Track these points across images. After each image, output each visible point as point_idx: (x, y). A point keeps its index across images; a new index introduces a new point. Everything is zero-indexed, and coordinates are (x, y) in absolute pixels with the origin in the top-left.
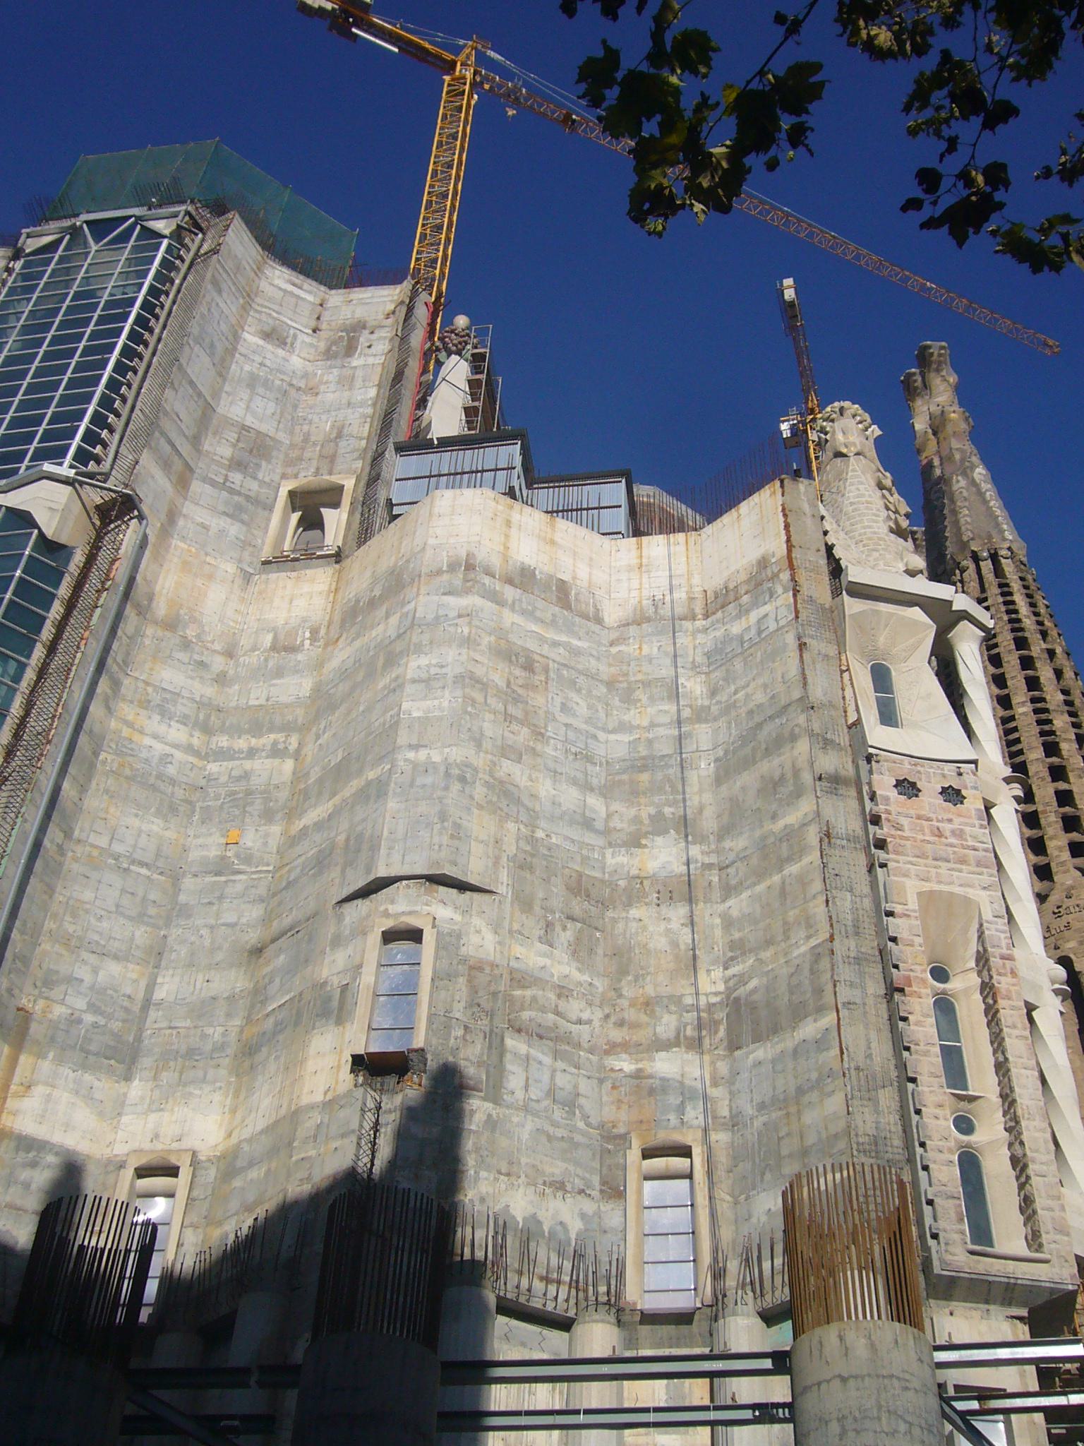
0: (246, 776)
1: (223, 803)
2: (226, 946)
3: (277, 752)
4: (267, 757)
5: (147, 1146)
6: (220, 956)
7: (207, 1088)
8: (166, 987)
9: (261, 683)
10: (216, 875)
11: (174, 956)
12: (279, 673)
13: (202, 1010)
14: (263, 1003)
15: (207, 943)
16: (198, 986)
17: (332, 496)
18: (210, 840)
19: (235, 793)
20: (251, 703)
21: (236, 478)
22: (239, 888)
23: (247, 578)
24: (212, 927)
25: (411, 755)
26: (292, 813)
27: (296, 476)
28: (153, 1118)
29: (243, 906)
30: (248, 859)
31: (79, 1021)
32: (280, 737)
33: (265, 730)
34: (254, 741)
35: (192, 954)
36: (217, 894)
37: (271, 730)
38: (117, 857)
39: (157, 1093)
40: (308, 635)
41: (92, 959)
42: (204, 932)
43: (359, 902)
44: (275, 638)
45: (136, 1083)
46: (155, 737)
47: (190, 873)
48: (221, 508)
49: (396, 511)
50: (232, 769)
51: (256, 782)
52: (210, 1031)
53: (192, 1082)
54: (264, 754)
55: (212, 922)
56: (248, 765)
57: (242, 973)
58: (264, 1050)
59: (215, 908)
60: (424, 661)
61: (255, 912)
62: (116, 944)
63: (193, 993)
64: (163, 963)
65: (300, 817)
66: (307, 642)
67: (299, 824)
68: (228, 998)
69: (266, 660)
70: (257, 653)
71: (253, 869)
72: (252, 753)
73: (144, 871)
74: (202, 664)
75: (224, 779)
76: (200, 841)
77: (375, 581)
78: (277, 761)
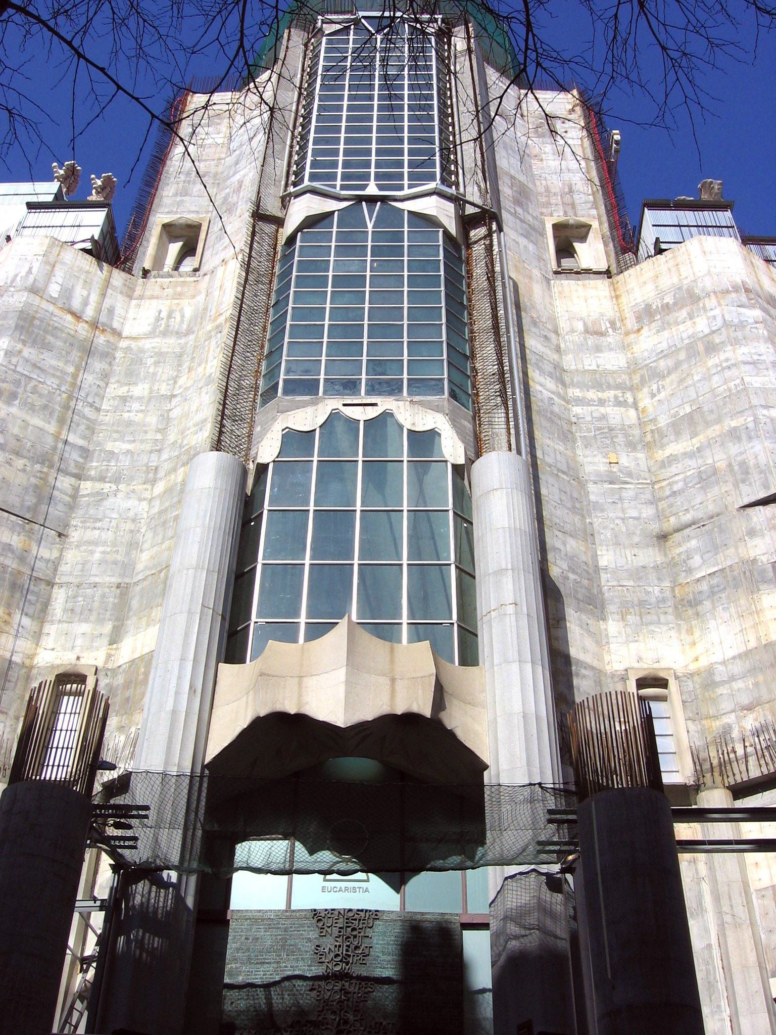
0: (604, 417)
1: (595, 435)
2: (638, 532)
3: (619, 403)
4: (614, 406)
5: (636, 665)
6: (636, 539)
7: (664, 628)
8: (605, 558)
9: (588, 355)
10: (611, 483)
11: (602, 537)
12: (598, 349)
13: (639, 573)
14: (690, 571)
15: (624, 529)
16: (629, 559)
17: (582, 231)
18: (596, 460)
19: (599, 429)
20: (587, 368)
21: (519, 210)
22: (631, 493)
23: (548, 281)
24: (623, 519)
25: (765, 412)
26: (648, 446)
27: (551, 215)
28: (633, 646)
29: (640, 506)
30: (629, 474)
31: (568, 578)
32: (619, 393)
33: (604, 387)
34: (600, 395)
35: (616, 536)
36: (617, 496)
37: (609, 387)
38: (550, 466)
39: (628, 630)
40: (608, 325)
41: (560, 534)
42: (617, 521)
43: (761, 507)
44: (585, 324)
45: (610, 622)
46: (541, 385)
47: (591, 481)
48: (521, 232)
49: (663, 246)
50: (592, 412)
51: (612, 422)
52: (650, 589)
53: (651, 623)
54: (610, 403)
55: (621, 515)
56: (602, 410)
57: (657, 551)
58: (707, 604)
59: (619, 506)
60: (744, 350)
61: (648, 512)
62: (569, 526)
63: (627, 563)
64: (597, 541)
65: (662, 447)
66: (610, 330)
67: (661, 455)
68: (654, 567)
69: (585, 339)
70: (575, 334)
71: (636, 482)
72: (602, 402)
73: (564, 477)
74: (546, 336)
75: (589, 418)
76: (589, 459)
77: (661, 294)
78: (623, 410)
